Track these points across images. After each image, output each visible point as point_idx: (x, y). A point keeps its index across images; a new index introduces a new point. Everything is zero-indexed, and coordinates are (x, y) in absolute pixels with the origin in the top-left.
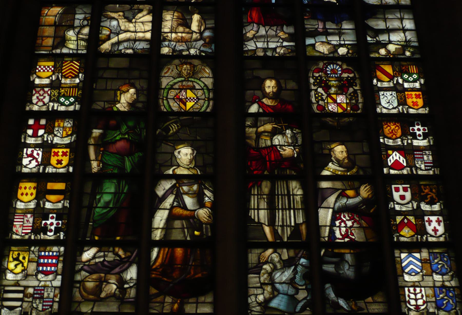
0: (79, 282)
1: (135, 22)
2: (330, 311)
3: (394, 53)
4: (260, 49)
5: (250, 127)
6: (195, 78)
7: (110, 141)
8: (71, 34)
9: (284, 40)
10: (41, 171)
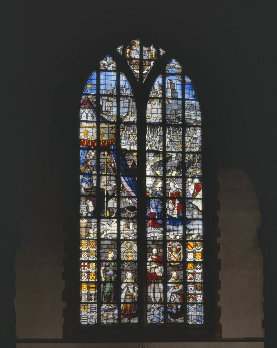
0: (102, 314)
2: (169, 322)
5: (148, 266)
8: (91, 231)
10: (88, 281)
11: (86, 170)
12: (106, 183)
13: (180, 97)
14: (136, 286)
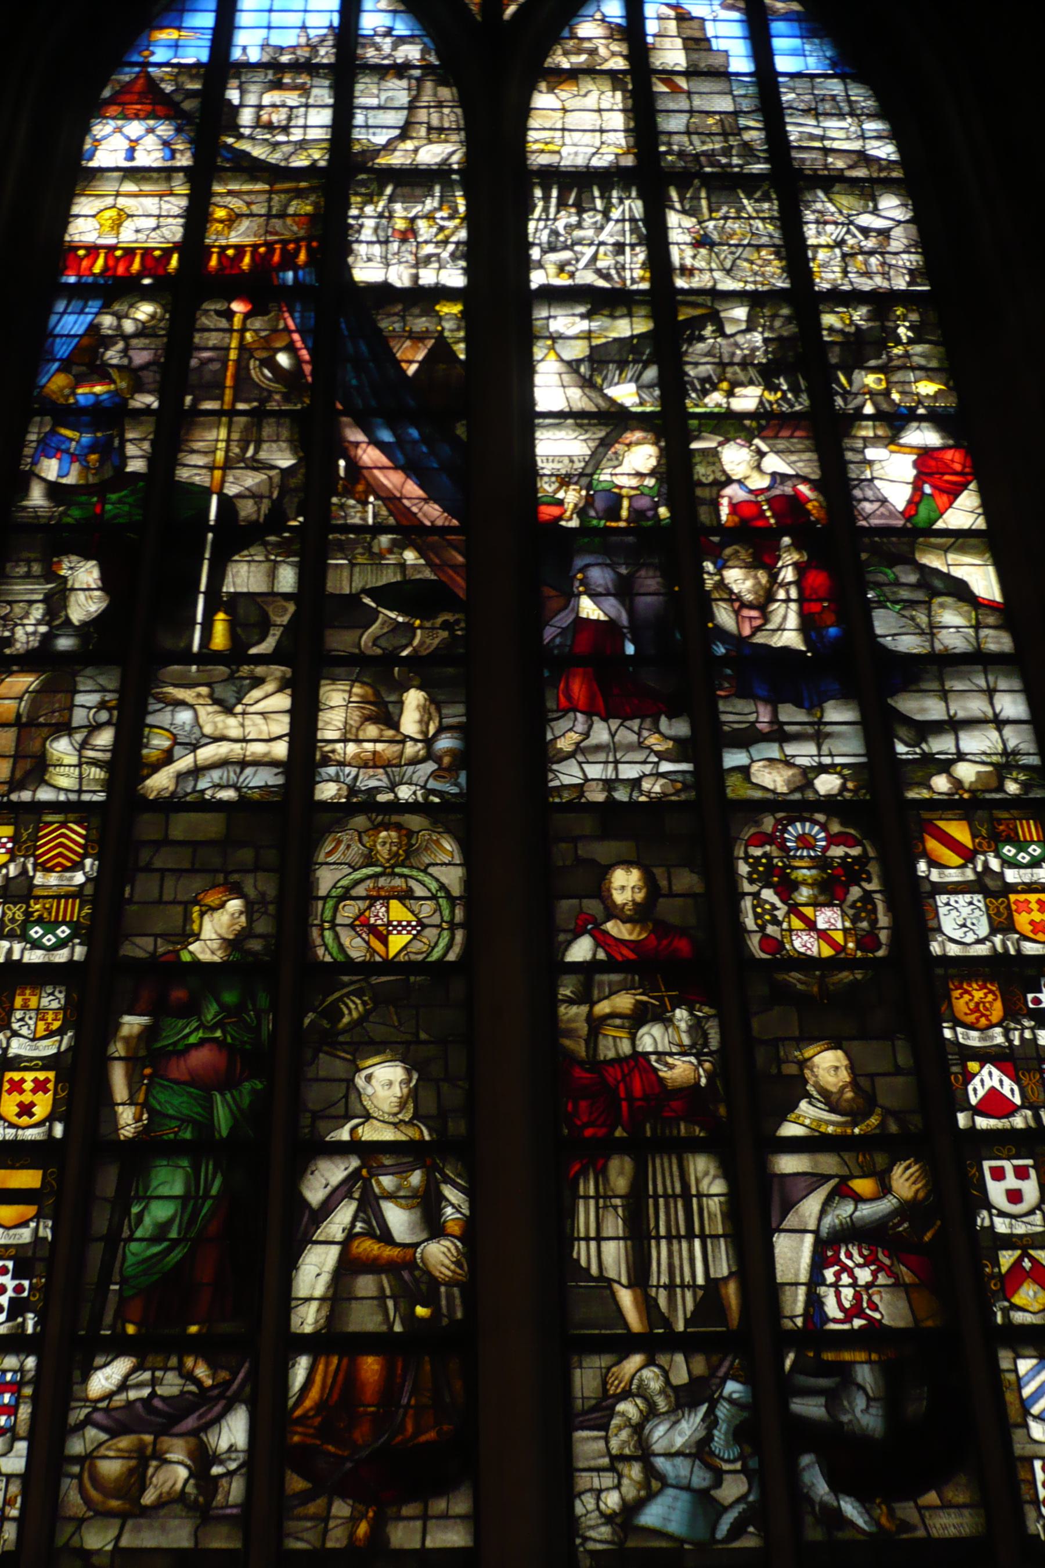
0: (80, 1460)
1: (244, 713)
2: (814, 1534)
3: (974, 787)
4: (594, 783)
5: (571, 1002)
6: (412, 867)
7: (171, 1048)
8: (62, 748)
9: (662, 756)
11: (80, 391)
12: (220, 455)
13: (741, 62)
14: (448, 1180)
